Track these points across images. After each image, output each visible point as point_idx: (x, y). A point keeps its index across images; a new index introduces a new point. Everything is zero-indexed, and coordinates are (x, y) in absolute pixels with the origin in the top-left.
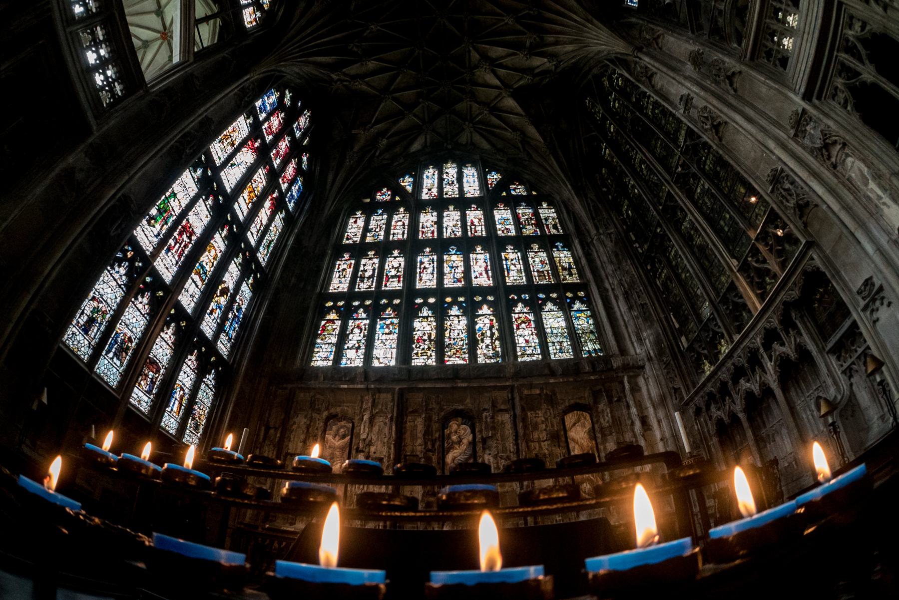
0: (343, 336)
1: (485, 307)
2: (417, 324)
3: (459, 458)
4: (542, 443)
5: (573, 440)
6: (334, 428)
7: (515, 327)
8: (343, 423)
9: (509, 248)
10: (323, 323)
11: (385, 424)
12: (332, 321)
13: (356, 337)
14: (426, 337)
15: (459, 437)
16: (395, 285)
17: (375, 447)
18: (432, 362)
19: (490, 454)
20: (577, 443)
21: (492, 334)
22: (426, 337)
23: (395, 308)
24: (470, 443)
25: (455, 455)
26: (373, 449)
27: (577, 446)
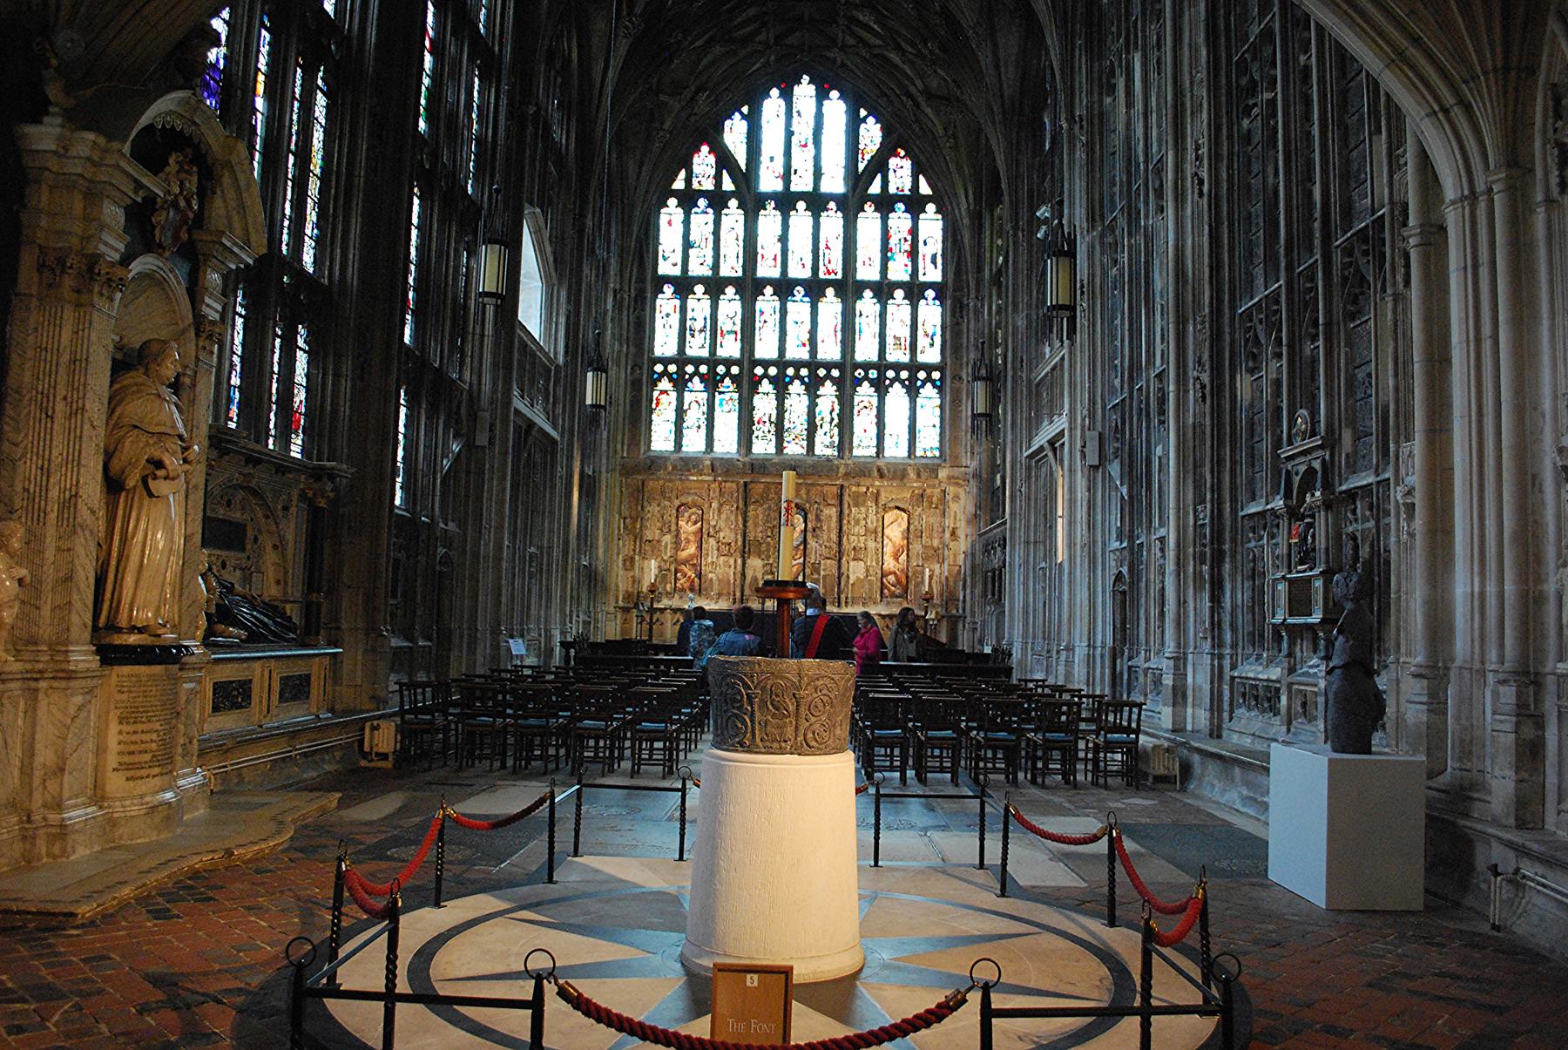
0: (680, 412)
1: (828, 383)
2: (757, 400)
6: (686, 515)
7: (855, 412)
8: (694, 510)
9: (868, 294)
10: (656, 394)
12: (663, 392)
13: (695, 416)
14: (766, 419)
16: (730, 348)
18: (772, 449)
21: (833, 419)
22: (766, 419)
23: (734, 379)
26: (722, 534)
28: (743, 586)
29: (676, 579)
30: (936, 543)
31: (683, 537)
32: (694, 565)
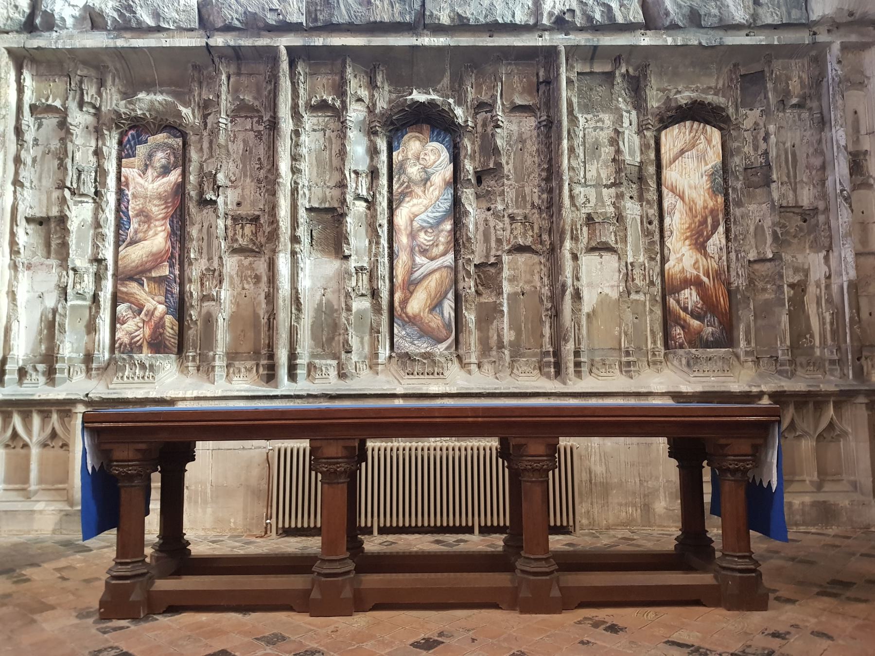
3: (423, 216)
4: (605, 191)
5: (673, 190)
6: (141, 150)
8: (161, 137)
11: (259, 135)
15: (424, 169)
17: (239, 190)
19: (489, 209)
20: (682, 198)
24: (447, 184)
25: (415, 210)
27: (680, 204)
28: (293, 332)
29: (115, 320)
30: (806, 197)
31: (133, 207)
32: (160, 280)
